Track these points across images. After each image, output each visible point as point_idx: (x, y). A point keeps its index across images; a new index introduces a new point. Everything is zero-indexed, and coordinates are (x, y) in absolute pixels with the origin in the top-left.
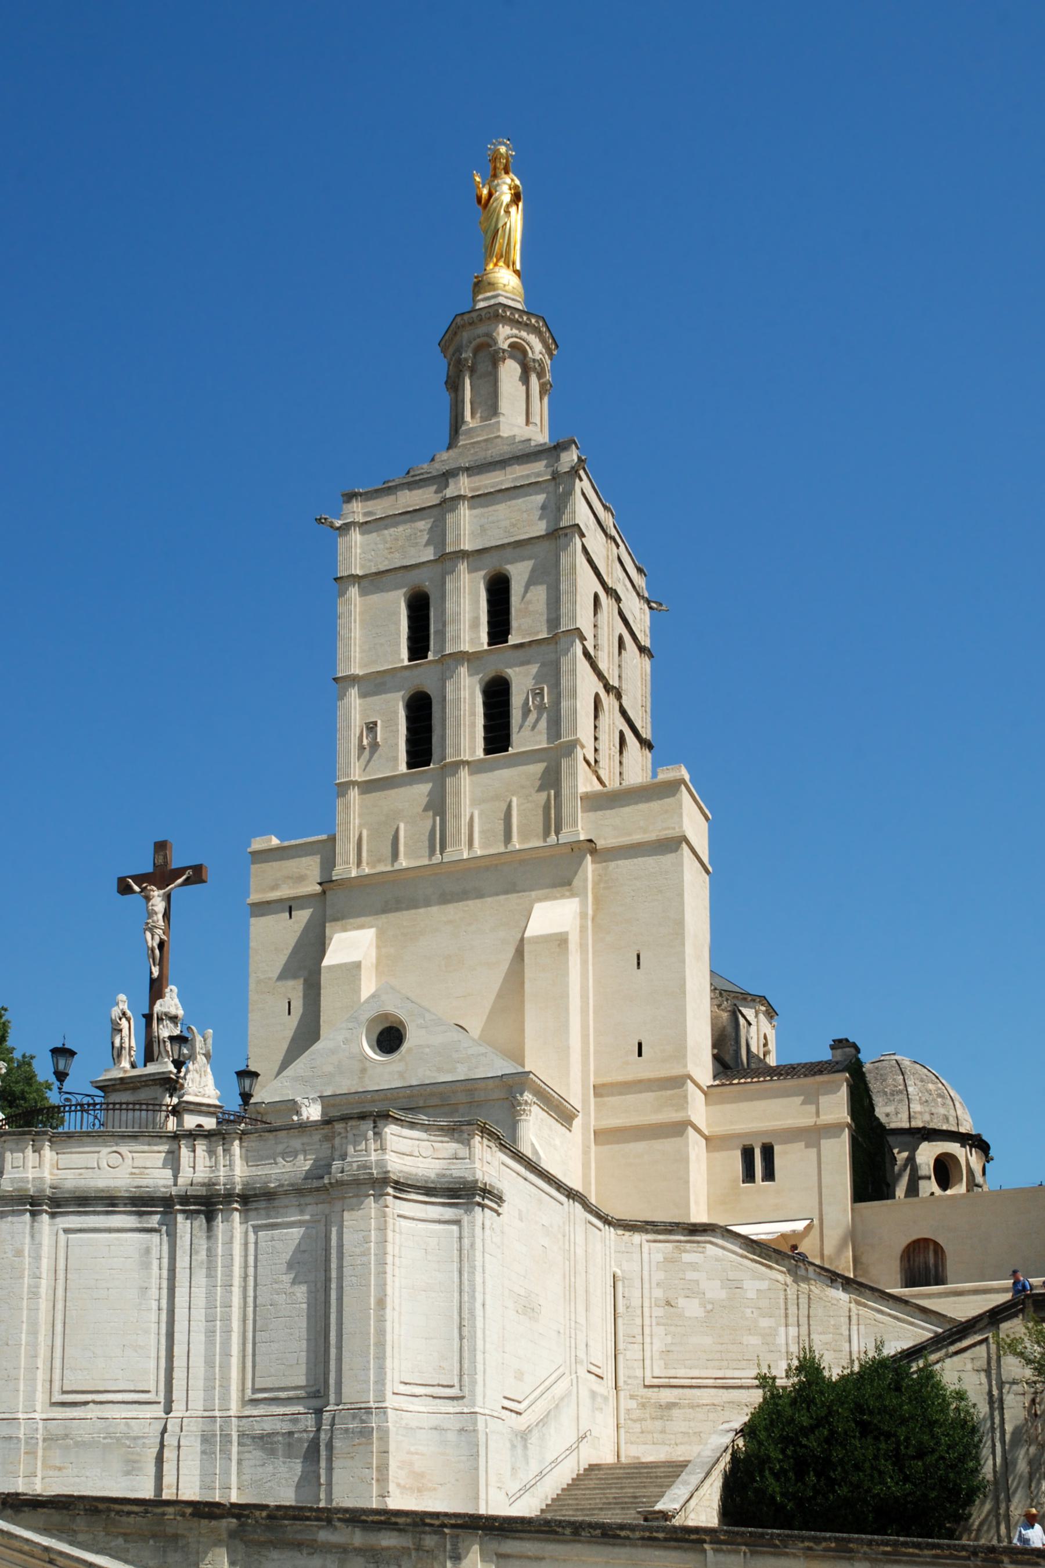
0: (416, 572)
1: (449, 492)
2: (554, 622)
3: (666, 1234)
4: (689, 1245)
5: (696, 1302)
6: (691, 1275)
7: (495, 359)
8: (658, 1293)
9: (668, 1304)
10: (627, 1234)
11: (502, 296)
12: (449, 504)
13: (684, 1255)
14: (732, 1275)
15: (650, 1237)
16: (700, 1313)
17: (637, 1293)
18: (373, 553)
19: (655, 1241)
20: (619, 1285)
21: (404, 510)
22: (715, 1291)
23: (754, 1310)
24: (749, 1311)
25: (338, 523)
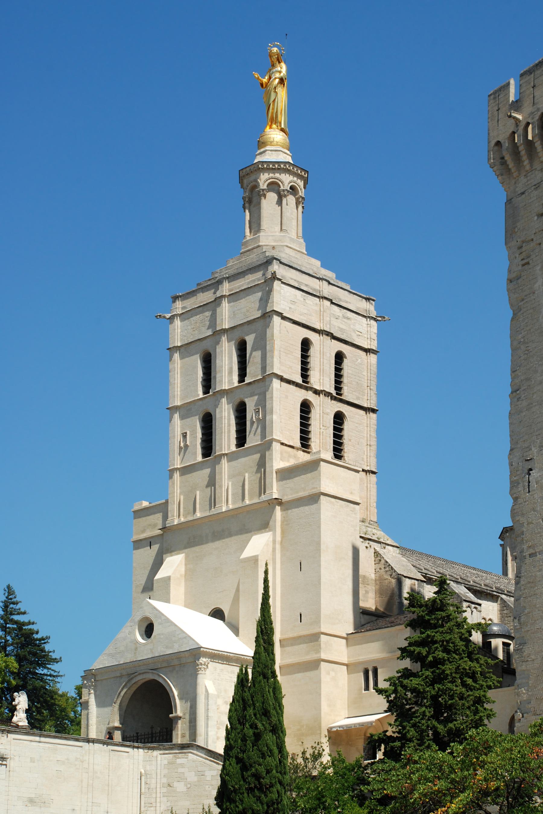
0: (205, 342)
1: (218, 294)
2: (264, 369)
3: (169, 750)
4: (181, 754)
5: (182, 784)
6: (181, 770)
7: (262, 194)
8: (165, 780)
9: (169, 785)
10: (150, 751)
11: (268, 150)
12: (218, 301)
13: (178, 760)
14: (200, 769)
15: (162, 752)
16: (184, 789)
17: (154, 781)
18: (186, 331)
19: (164, 754)
20: (143, 778)
21: (199, 305)
22: (192, 777)
23: (210, 786)
24: (207, 786)
25: (168, 316)
